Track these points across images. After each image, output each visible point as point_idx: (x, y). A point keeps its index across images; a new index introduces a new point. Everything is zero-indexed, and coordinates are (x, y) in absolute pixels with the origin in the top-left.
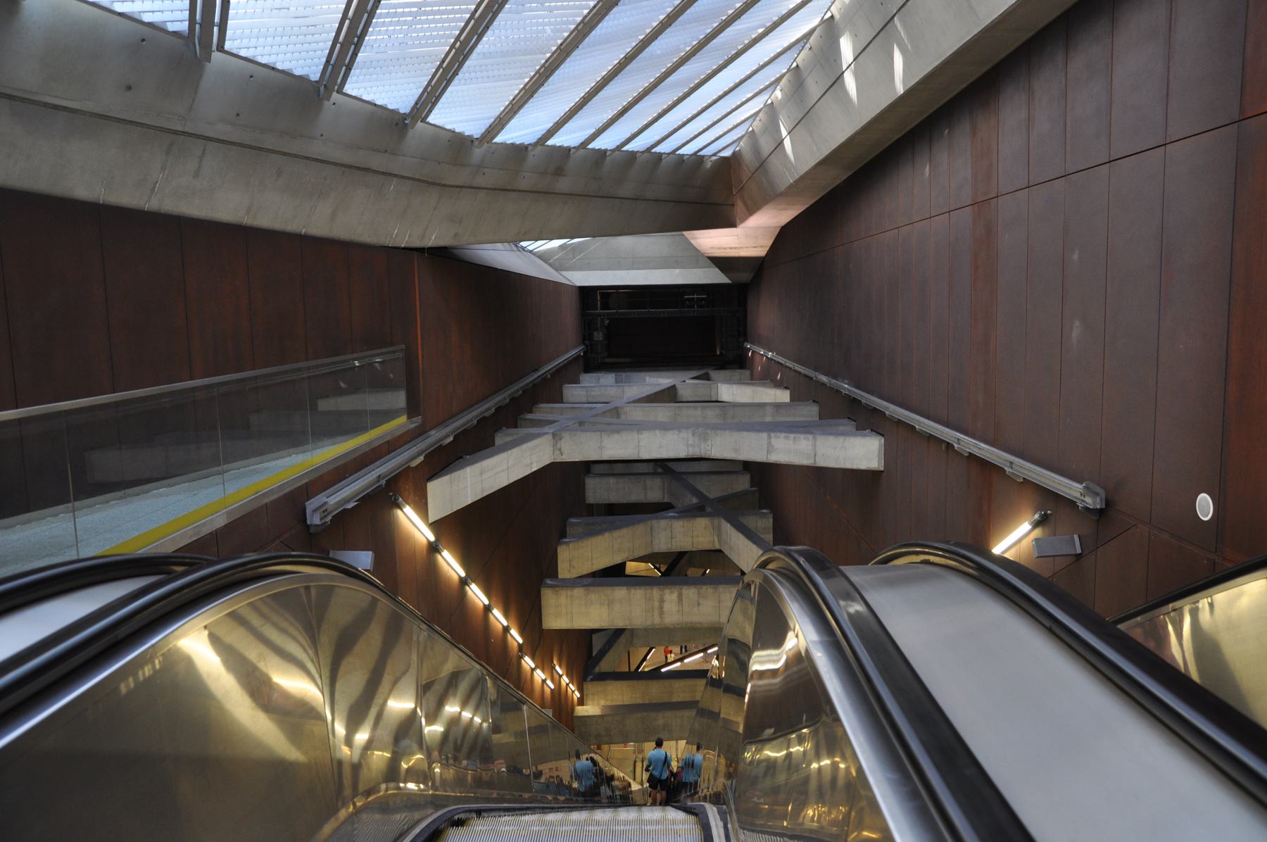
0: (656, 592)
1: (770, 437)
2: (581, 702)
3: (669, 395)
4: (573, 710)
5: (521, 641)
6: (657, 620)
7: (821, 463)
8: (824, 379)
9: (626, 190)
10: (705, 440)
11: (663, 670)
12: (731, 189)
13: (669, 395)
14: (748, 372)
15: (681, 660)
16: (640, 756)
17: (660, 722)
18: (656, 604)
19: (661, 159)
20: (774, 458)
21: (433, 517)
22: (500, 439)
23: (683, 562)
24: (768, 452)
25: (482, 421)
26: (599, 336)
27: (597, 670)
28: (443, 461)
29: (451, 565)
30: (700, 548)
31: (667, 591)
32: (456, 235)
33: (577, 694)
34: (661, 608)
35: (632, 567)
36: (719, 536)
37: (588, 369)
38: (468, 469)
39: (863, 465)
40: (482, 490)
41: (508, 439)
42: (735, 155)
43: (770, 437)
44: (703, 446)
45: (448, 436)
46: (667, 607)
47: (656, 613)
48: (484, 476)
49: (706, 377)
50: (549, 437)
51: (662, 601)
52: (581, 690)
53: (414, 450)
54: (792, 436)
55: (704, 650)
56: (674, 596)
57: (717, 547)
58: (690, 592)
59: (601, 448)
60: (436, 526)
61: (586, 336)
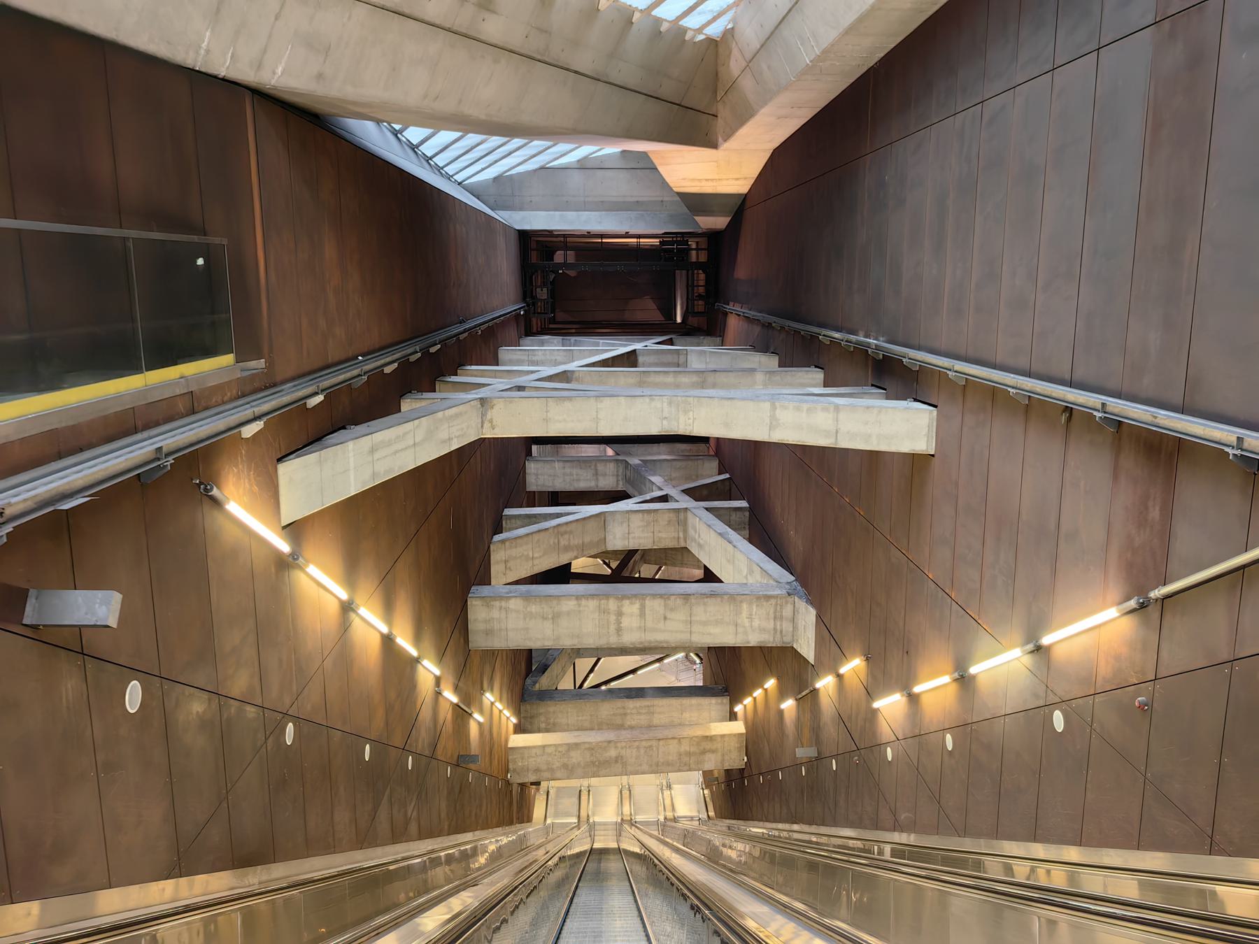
0: (612, 605)
1: (774, 408)
2: (519, 729)
3: (630, 359)
4: (507, 741)
6: (613, 641)
7: (844, 444)
8: (837, 335)
9: (585, 61)
10: (686, 412)
11: (613, 684)
12: (715, 92)
13: (630, 359)
14: (718, 340)
15: (633, 671)
17: (613, 753)
18: (613, 618)
19: (630, 23)
20: (777, 436)
21: (289, 514)
22: (407, 405)
23: (637, 557)
24: (772, 427)
25: (377, 375)
26: (542, 294)
28: (309, 431)
29: (321, 583)
30: (662, 546)
32: (320, 76)
34: (619, 622)
35: (579, 566)
36: (685, 531)
37: (529, 333)
38: (351, 445)
39: (906, 447)
40: (374, 475)
41: (417, 405)
42: (729, 34)
43: (774, 408)
44: (682, 418)
45: (316, 394)
46: (626, 622)
47: (613, 628)
48: (377, 456)
49: (670, 342)
50: (477, 403)
51: (620, 614)
52: (517, 712)
53: (248, 413)
54: (805, 406)
56: (635, 608)
57: (683, 545)
59: (546, 420)
60: (294, 530)
61: (527, 293)
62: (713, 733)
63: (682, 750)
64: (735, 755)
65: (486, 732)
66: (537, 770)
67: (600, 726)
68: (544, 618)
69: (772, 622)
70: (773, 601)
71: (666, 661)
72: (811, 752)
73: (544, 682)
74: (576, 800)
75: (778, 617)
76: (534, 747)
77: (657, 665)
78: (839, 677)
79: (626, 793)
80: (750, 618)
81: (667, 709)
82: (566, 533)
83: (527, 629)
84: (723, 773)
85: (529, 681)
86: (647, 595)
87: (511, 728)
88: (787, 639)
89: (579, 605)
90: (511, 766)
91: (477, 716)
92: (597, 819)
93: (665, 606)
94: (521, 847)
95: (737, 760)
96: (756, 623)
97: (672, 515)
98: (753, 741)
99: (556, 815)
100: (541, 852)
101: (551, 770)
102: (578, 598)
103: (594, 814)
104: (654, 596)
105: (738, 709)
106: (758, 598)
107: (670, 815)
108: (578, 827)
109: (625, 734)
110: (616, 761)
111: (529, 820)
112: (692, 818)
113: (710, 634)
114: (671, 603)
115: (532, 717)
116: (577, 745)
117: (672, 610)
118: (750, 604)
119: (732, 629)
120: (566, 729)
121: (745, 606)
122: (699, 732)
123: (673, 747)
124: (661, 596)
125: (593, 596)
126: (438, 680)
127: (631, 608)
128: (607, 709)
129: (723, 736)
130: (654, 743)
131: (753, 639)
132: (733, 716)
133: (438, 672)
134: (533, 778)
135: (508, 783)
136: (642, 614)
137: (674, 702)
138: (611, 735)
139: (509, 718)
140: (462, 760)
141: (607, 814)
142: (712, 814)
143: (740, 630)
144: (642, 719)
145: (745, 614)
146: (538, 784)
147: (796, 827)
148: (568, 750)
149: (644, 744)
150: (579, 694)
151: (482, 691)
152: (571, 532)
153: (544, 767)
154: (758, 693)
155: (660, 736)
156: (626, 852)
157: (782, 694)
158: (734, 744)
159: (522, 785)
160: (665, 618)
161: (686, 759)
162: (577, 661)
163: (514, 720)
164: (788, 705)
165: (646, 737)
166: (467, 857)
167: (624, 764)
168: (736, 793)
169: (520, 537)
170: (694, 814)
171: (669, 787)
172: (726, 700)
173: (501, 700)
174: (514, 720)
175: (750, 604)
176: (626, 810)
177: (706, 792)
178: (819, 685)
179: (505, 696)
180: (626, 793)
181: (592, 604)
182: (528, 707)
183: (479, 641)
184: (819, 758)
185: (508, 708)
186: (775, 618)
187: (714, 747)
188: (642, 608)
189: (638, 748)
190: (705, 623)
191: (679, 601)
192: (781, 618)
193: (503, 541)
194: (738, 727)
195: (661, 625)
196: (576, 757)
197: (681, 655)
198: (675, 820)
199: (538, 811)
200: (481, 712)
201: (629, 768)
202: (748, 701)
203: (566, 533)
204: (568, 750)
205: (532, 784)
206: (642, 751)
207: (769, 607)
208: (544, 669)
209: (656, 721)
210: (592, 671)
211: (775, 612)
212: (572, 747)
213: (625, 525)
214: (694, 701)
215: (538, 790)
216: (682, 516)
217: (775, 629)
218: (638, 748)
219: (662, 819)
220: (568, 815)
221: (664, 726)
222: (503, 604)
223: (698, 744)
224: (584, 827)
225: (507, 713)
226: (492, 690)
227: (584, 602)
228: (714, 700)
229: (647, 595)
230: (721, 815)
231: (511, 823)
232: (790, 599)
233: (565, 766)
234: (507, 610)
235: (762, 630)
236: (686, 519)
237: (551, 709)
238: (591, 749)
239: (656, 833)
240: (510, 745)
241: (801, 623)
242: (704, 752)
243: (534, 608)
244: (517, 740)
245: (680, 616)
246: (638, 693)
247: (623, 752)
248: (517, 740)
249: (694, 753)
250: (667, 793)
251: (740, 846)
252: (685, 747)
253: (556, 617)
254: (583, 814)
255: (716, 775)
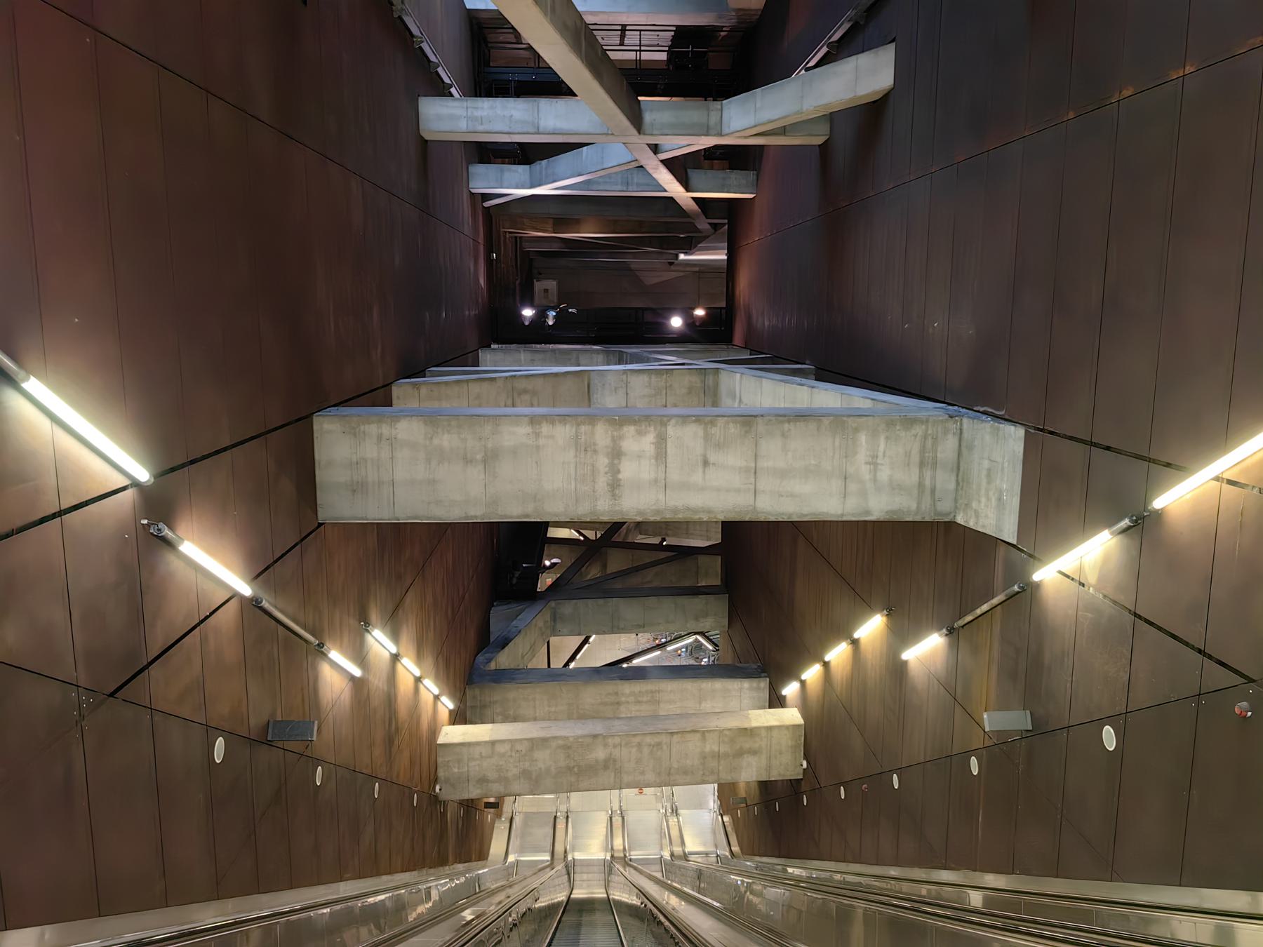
2: (458, 718)
4: (434, 732)
5: (143, 475)
14: (751, 175)
16: (563, 808)
17: (600, 754)
18: (603, 462)
27: (493, 666)
31: (630, 430)
33: (448, 704)
34: (614, 470)
46: (628, 470)
47: (602, 482)
51: (616, 454)
55: (660, 646)
58: (686, 438)
62: (754, 724)
63: (708, 749)
64: (787, 758)
65: (377, 701)
66: (483, 780)
67: (583, 717)
68: (468, 461)
69: (915, 471)
70: (919, 430)
71: (669, 648)
72: (1017, 720)
73: (504, 660)
74: (550, 830)
75: (927, 462)
76: (478, 744)
77: (658, 653)
78: (1142, 525)
79: (617, 820)
80: (873, 463)
81: (679, 697)
82: (525, 391)
83: (432, 482)
84: (755, 787)
85: (480, 658)
86: (671, 417)
87: (444, 714)
88: (945, 506)
89: (537, 435)
90: (441, 773)
91: (334, 655)
92: (578, 856)
93: (707, 438)
94: (473, 893)
95: (788, 765)
96: (884, 474)
97: (696, 380)
98: (820, 734)
99: (522, 850)
100: (501, 897)
101: (505, 780)
102: (534, 420)
103: (573, 850)
104: (684, 419)
105: (790, 690)
106: (890, 424)
107: (678, 850)
108: (551, 865)
109: (618, 726)
110: (606, 767)
111: (482, 855)
112: (707, 854)
113: (792, 495)
114: (716, 431)
115: (484, 707)
116: (544, 741)
117: (719, 446)
118: (874, 434)
119: (836, 485)
120: (535, 719)
121: (863, 438)
122: (733, 723)
123: (694, 745)
124: (698, 419)
125: (563, 418)
126: (158, 506)
127: (638, 443)
128: (592, 695)
129: (770, 728)
130: (664, 739)
131: (878, 507)
132: (776, 701)
133: (143, 475)
134: (473, 793)
135: (435, 800)
136: (661, 454)
137: (690, 686)
138: (597, 727)
139: (420, 684)
140: (281, 738)
141: (592, 848)
142: (736, 849)
143: (852, 487)
144: (645, 709)
145: (862, 455)
146: (495, 805)
147: (946, 875)
148: (531, 749)
149: (648, 739)
150: (551, 675)
151: (365, 622)
152: (534, 393)
153: (492, 775)
154: (838, 654)
155: (674, 728)
156: (619, 904)
157: (902, 633)
158: (786, 741)
159: (469, 806)
160: (706, 463)
161: (713, 764)
162: (553, 640)
163: (448, 703)
164: (927, 650)
165: (651, 729)
166: (400, 907)
167: (618, 772)
168: (777, 817)
169: (446, 383)
170: (712, 849)
171: (675, 812)
172: (764, 684)
173: (419, 659)
174: (448, 703)
175: (874, 434)
176: (618, 843)
177: (726, 819)
178: (1047, 574)
179: (429, 661)
180: (617, 820)
181: (563, 433)
182: (477, 691)
183: (338, 505)
184: (1040, 730)
185: (437, 680)
186: (922, 464)
187: (757, 745)
188: (661, 441)
189: (639, 745)
190: (783, 474)
191: (733, 429)
192: (934, 464)
193: (414, 384)
194: (791, 716)
195: (697, 477)
196: (543, 759)
197: (690, 640)
198: (685, 857)
199: (497, 846)
200: (360, 656)
201: (626, 779)
202: (812, 673)
203: (525, 391)
204: (531, 749)
205: (489, 805)
206: (646, 750)
207: (909, 441)
208: (504, 643)
209: (664, 709)
210: (572, 658)
211: (923, 450)
212: (536, 744)
213: (622, 392)
214: (719, 684)
215: (499, 816)
216: (710, 380)
217: (921, 485)
218: (639, 745)
219: (667, 855)
220: (537, 849)
221: (681, 716)
222: (385, 430)
223: (732, 741)
224: (560, 867)
225: (431, 686)
226: (395, 637)
227: (545, 429)
228: (746, 684)
229: (671, 417)
230: (750, 849)
231: (442, 861)
232: (952, 425)
233: (526, 774)
234: (392, 441)
235: (895, 487)
236: (717, 385)
237: (512, 695)
238: (567, 747)
239: (659, 875)
240: (441, 740)
241: (978, 465)
242: (740, 753)
243: (447, 440)
244: (452, 734)
245: (735, 458)
246: (641, 674)
247: (616, 752)
248: (452, 734)
249: (726, 755)
250: (673, 821)
251: (775, 892)
252: (712, 746)
253: (490, 458)
254: (559, 848)
255: (742, 793)
